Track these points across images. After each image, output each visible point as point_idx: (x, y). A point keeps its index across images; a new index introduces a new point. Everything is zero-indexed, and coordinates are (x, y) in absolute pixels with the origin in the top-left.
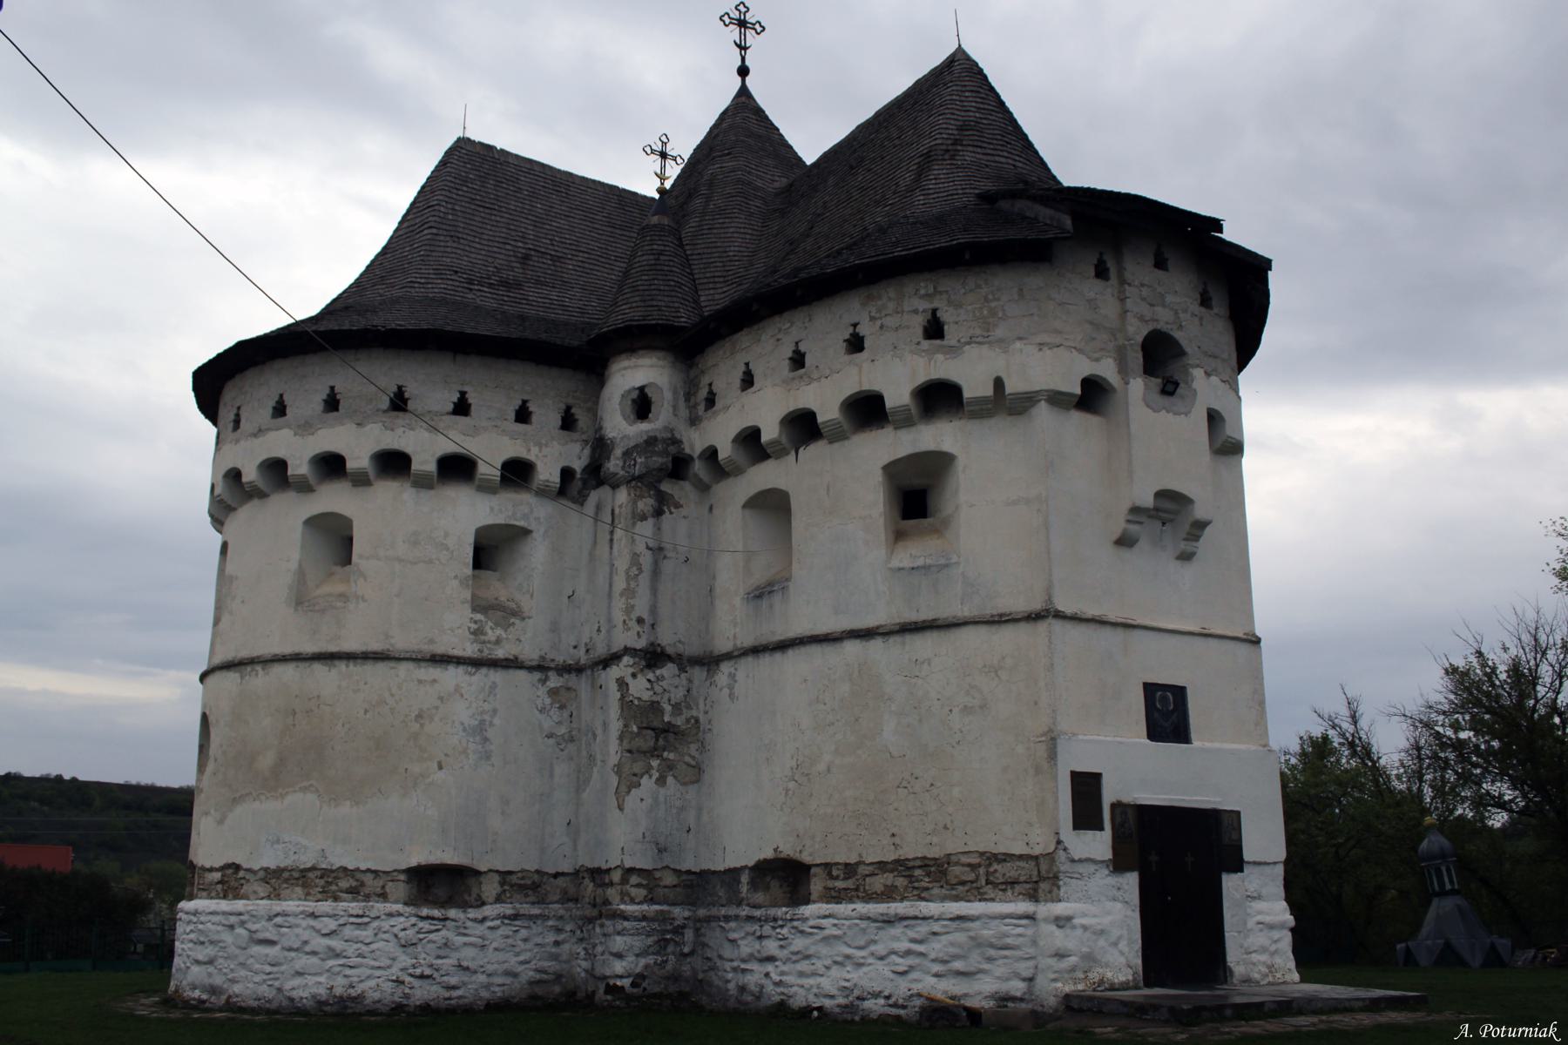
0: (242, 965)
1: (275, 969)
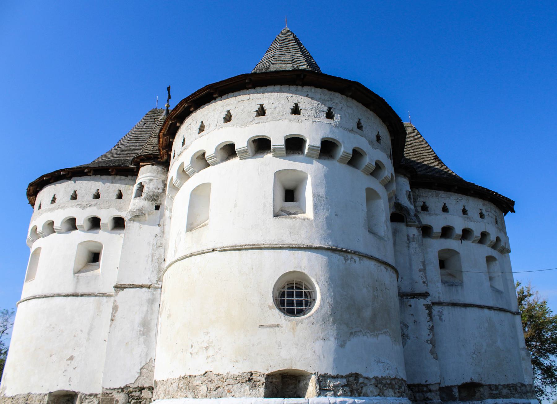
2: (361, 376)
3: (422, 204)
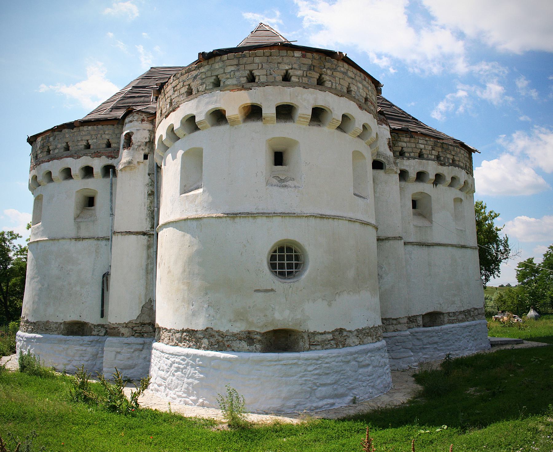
0: (356, 380)
1: (371, 377)
2: (345, 330)
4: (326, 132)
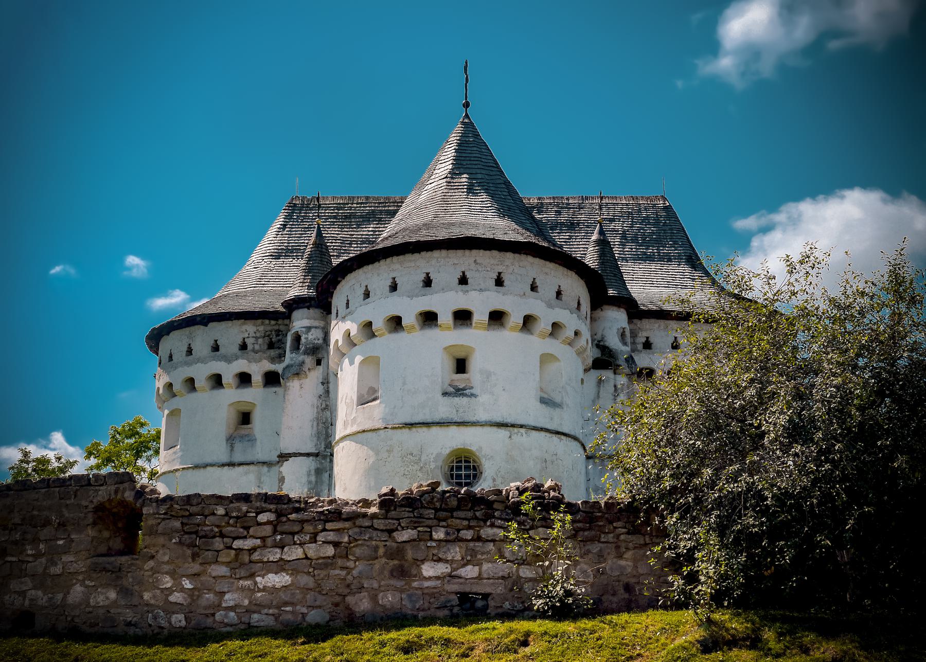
3: (644, 340)
4: (508, 336)
